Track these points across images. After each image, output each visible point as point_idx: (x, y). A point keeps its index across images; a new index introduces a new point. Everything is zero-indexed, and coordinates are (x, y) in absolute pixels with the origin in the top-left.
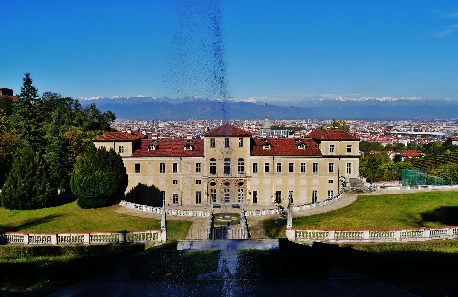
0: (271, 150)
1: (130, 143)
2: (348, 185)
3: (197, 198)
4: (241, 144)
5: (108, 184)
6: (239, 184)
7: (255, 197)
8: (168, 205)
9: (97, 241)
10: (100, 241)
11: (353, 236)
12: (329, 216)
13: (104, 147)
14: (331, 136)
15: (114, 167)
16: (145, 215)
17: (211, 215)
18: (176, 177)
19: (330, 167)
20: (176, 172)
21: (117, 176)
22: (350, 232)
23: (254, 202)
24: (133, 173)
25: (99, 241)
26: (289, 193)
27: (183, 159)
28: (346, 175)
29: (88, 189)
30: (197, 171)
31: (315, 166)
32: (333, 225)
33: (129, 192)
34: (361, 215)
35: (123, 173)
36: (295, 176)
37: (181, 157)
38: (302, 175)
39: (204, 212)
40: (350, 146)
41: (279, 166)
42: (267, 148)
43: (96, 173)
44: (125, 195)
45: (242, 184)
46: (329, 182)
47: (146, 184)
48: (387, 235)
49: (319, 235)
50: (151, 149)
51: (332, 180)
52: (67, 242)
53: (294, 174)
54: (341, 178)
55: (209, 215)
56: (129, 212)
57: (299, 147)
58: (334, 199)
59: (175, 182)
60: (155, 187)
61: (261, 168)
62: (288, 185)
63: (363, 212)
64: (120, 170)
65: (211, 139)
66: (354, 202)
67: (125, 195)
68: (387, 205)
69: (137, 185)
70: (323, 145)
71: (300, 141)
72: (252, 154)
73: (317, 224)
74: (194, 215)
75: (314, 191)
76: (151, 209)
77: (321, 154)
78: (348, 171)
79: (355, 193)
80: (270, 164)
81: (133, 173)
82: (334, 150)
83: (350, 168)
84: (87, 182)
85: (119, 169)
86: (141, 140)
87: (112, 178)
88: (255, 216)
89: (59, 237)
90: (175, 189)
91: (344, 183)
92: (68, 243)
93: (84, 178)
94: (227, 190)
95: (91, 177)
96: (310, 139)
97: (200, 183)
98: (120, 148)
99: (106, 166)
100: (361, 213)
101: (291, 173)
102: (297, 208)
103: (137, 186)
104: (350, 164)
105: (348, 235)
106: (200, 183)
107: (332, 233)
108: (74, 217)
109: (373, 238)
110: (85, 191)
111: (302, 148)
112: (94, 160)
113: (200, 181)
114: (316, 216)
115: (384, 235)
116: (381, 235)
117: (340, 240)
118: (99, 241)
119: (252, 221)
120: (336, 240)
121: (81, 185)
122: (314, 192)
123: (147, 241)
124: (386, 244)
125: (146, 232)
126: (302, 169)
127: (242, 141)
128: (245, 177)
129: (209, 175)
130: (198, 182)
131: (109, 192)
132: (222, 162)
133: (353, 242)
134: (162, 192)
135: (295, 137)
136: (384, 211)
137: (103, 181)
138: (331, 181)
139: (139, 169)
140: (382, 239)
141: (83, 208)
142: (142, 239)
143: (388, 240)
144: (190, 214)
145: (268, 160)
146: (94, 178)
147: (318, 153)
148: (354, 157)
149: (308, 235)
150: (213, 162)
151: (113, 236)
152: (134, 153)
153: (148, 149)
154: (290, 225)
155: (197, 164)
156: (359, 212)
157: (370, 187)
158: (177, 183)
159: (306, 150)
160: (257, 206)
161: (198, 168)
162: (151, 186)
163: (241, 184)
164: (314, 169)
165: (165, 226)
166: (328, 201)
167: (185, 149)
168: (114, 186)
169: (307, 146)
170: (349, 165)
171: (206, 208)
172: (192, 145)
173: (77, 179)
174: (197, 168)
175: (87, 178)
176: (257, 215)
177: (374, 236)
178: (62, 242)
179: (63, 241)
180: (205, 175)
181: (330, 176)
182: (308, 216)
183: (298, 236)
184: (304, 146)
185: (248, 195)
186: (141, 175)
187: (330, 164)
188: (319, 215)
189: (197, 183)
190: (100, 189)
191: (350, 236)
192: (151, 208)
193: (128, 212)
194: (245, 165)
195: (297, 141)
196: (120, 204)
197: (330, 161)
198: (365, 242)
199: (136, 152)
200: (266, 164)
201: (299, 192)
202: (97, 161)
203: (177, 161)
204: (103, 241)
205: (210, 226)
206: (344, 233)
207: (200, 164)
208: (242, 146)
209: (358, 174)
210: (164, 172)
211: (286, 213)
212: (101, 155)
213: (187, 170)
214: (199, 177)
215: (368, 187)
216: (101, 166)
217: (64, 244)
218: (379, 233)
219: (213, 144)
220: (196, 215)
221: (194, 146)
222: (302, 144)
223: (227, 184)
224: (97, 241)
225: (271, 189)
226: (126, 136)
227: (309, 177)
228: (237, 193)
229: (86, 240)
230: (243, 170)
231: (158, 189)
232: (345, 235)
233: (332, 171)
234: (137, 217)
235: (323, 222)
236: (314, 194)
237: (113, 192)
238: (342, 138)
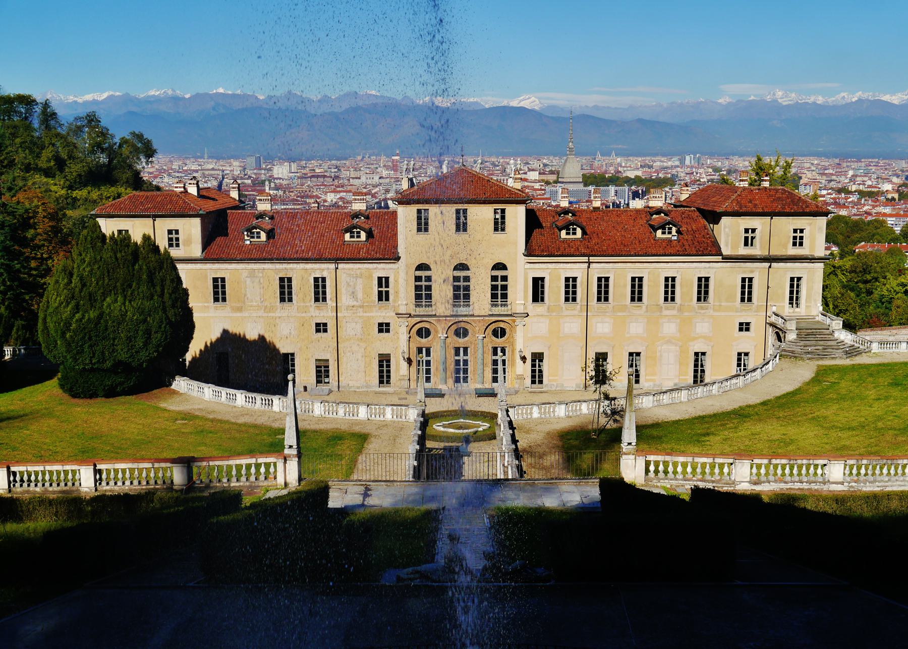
0: (581, 242)
1: (197, 222)
2: (791, 336)
3: (381, 372)
4: (499, 225)
5: (140, 333)
6: (495, 333)
7: (537, 368)
8: (302, 389)
9: (116, 483)
10: (124, 483)
11: (800, 474)
12: (735, 421)
13: (128, 231)
14: (750, 202)
15: (154, 286)
16: (243, 415)
17: (418, 415)
18: (324, 314)
19: (743, 287)
20: (324, 299)
21: (164, 310)
22: (792, 462)
23: (533, 382)
24: (206, 305)
25: (120, 483)
26: (631, 358)
27: (340, 266)
28: (787, 310)
29: (87, 345)
30: (380, 299)
31: (703, 286)
32: (747, 443)
33: (198, 356)
34: (825, 418)
35: (179, 304)
36: (647, 311)
37: (337, 260)
38: (667, 309)
39: (399, 407)
40: (802, 231)
41: (603, 286)
42: (571, 236)
43: (105, 304)
44: (187, 363)
45: (503, 332)
46: (741, 330)
47: (242, 336)
48: (892, 471)
49: (707, 470)
50: (253, 237)
51: (748, 324)
52: (36, 485)
53: (644, 307)
54: (773, 319)
55: (413, 415)
56: (199, 407)
57: (659, 233)
58: (753, 374)
59: (321, 328)
60: (268, 340)
61: (554, 290)
62: (627, 336)
63: (830, 411)
64: (170, 295)
65: (419, 211)
66: (808, 384)
67: (187, 363)
68: (896, 392)
69: (219, 335)
70: (725, 227)
71: (662, 215)
72: (529, 252)
73: (703, 441)
74: (373, 416)
75: (696, 354)
76: (259, 401)
77: (720, 253)
78: (794, 299)
79: (809, 359)
80: (578, 280)
81: (206, 305)
82: (756, 241)
83: (797, 292)
84: (84, 328)
85: (169, 293)
86: (227, 214)
87: (150, 316)
88: (538, 418)
89: (14, 474)
90: (323, 347)
91: (780, 333)
92: (38, 489)
93: (74, 315)
94: (462, 350)
95: (92, 314)
96: (690, 211)
97: (388, 331)
98: (170, 236)
99: (134, 284)
100: (823, 412)
101: (636, 304)
102: (651, 397)
103: (218, 340)
104: (799, 279)
105: (787, 471)
106: (388, 331)
107: (743, 466)
108: (52, 422)
109: (856, 478)
110: (77, 353)
111: (667, 236)
112: (99, 268)
113: (388, 325)
114: (701, 419)
115: (885, 471)
116: (877, 472)
117: (764, 482)
118: (120, 483)
119: (528, 431)
120: (755, 483)
121: (68, 336)
122: (699, 356)
123: (248, 484)
124: (889, 496)
125: (244, 461)
126: (666, 292)
127: (503, 217)
128: (511, 315)
129: (412, 309)
130: (384, 328)
131: (143, 355)
132: (450, 273)
133: (799, 489)
134: (286, 355)
135: (650, 205)
136: (888, 407)
137: (127, 325)
138: (744, 327)
139: (224, 293)
140: (879, 482)
141: (75, 396)
142: (234, 479)
143: (895, 486)
144: (363, 412)
145: (575, 268)
146: (102, 318)
147: (712, 248)
148: (811, 259)
149: (679, 469)
150: (423, 274)
151: (156, 471)
152: (209, 248)
153: (246, 238)
154: (630, 444)
155: (380, 279)
156: (819, 411)
157: (852, 343)
158: (325, 331)
159: (678, 241)
160: (541, 392)
161: (384, 289)
162: (255, 337)
163: (500, 333)
164: (699, 292)
165: (294, 442)
166: (734, 381)
167: (347, 236)
168: (156, 338)
169: (683, 229)
170: (795, 283)
171: (406, 399)
172: (367, 227)
173: (54, 319)
174: (380, 289)
175: (83, 316)
176: (543, 416)
177: (859, 474)
178: (21, 486)
179: (25, 485)
180: (403, 310)
181: (744, 313)
182: (680, 420)
183: (652, 472)
184: (674, 229)
185: (519, 361)
186: (228, 308)
187: (743, 280)
188: (710, 416)
189: (380, 331)
190: (119, 347)
191: (791, 474)
192: (258, 397)
193: (196, 407)
194: (510, 283)
195: (654, 216)
196: (173, 387)
197: (745, 272)
198: (831, 489)
199: (213, 246)
200: (567, 279)
201: (658, 354)
202: (108, 272)
203: (325, 269)
204: (132, 483)
205: (415, 444)
206: (776, 466)
207: (387, 279)
208: (503, 230)
209: (821, 308)
210: (290, 300)
211: (621, 411)
212: (119, 255)
213: (353, 294)
214: (385, 314)
215: (846, 341)
216: (118, 284)
217: (28, 492)
218: (870, 467)
219: (422, 225)
220: (378, 416)
221: (371, 228)
222: (669, 223)
223: (461, 333)
224: (116, 483)
225: (581, 348)
226: (185, 202)
227: (686, 314)
228: (489, 358)
229: (86, 480)
230: (505, 296)
231: (274, 346)
232: (779, 471)
233: (750, 300)
234: (220, 421)
235: (719, 435)
236: (696, 360)
237: (155, 354)
238: (779, 208)
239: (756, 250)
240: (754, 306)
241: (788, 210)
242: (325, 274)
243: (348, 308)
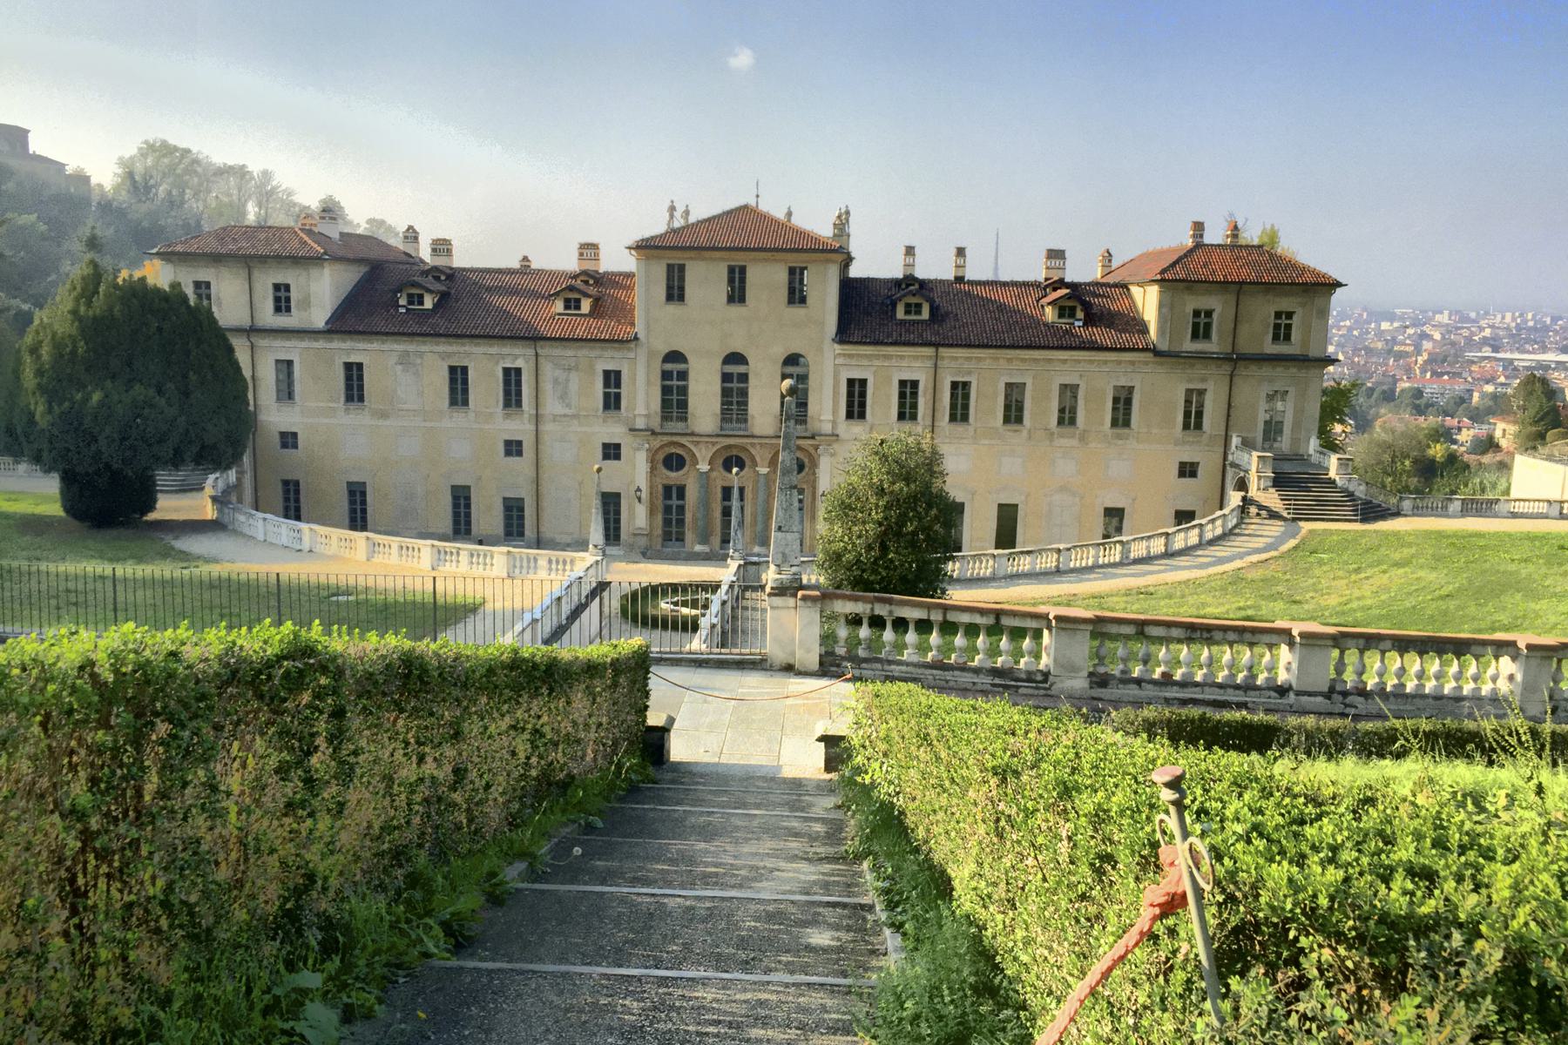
4: (796, 296)
18: (518, 427)
20: (519, 404)
30: (607, 406)
31: (1122, 407)
38: (1061, 436)
41: (960, 391)
53: (1025, 433)
59: (513, 448)
90: (516, 477)
113: (618, 446)
128: (813, 437)
139: (361, 388)
155: (607, 374)
158: (520, 453)
161: (613, 390)
180: (640, 423)
187: (1189, 392)
200: (902, 383)
203: (519, 357)
239: (1213, 346)
240: (1205, 436)
241: (1266, 279)
242: (519, 363)
243: (555, 418)
